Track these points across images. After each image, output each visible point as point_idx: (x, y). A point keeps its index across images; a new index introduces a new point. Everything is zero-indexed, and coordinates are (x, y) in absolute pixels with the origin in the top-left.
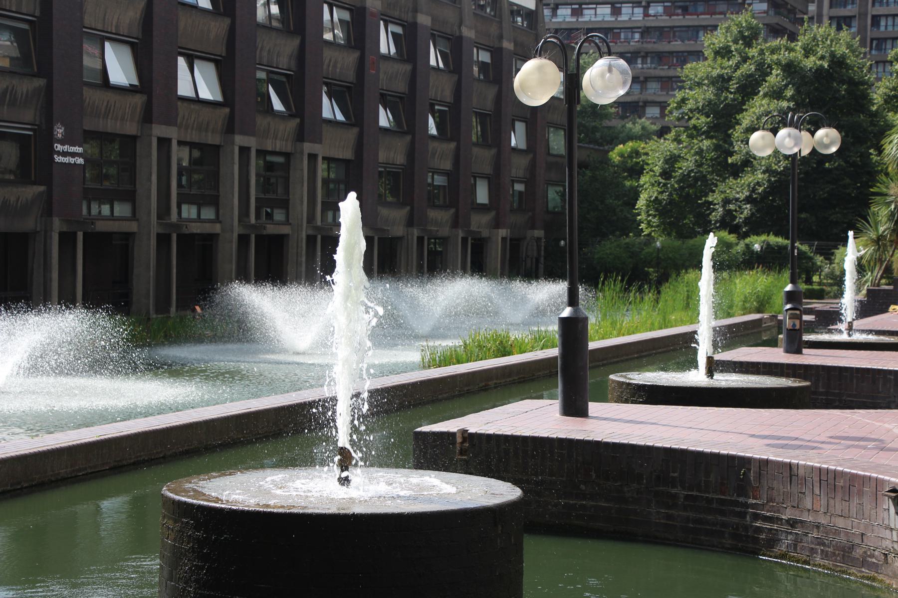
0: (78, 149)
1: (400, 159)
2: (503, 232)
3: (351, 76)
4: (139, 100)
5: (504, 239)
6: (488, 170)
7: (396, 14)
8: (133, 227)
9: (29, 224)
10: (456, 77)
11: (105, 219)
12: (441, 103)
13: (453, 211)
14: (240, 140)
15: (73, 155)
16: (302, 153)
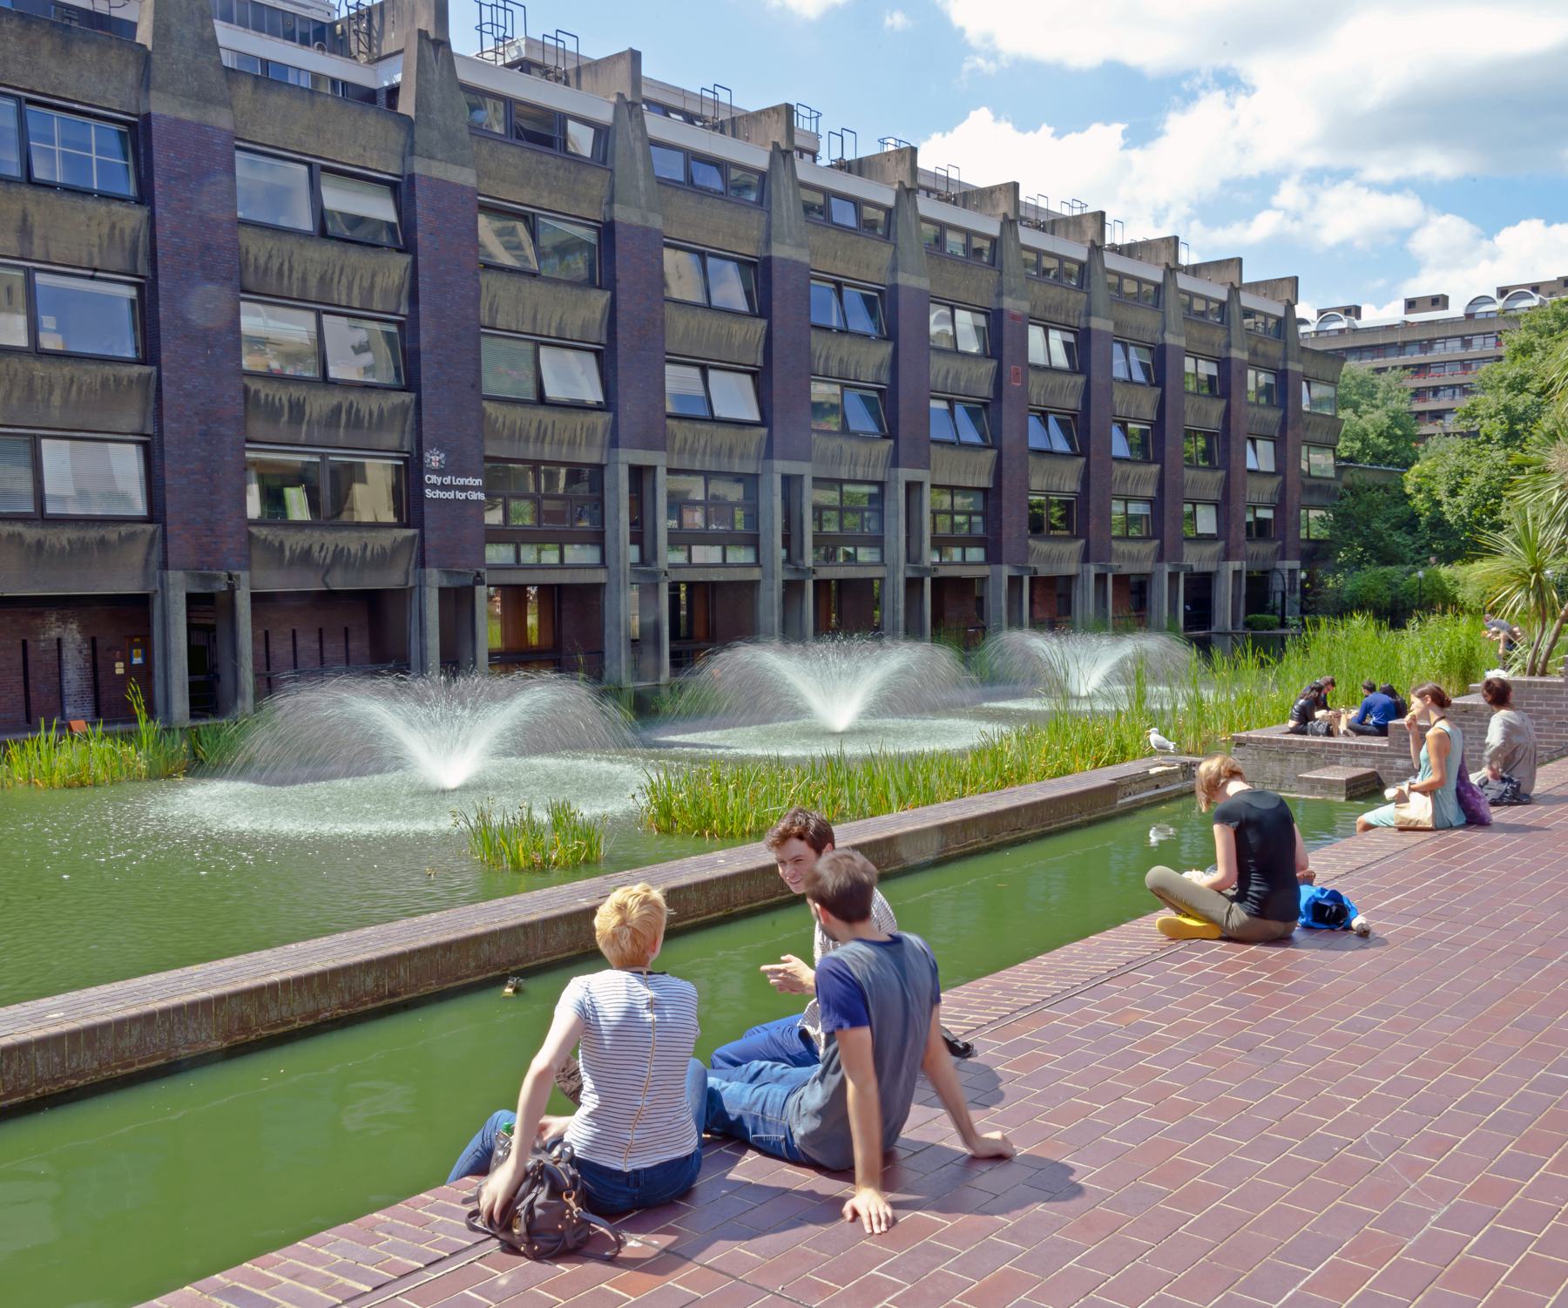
0: (478, 482)
1: (1071, 485)
2: (1235, 565)
3: (986, 390)
4: (601, 420)
5: (1237, 573)
6: (1215, 495)
7: (1061, 318)
8: (755, 574)
9: (391, 579)
10: (1158, 391)
11: (530, 567)
12: (1137, 420)
13: (1156, 542)
14: (781, 466)
15: (464, 488)
16: (896, 480)
